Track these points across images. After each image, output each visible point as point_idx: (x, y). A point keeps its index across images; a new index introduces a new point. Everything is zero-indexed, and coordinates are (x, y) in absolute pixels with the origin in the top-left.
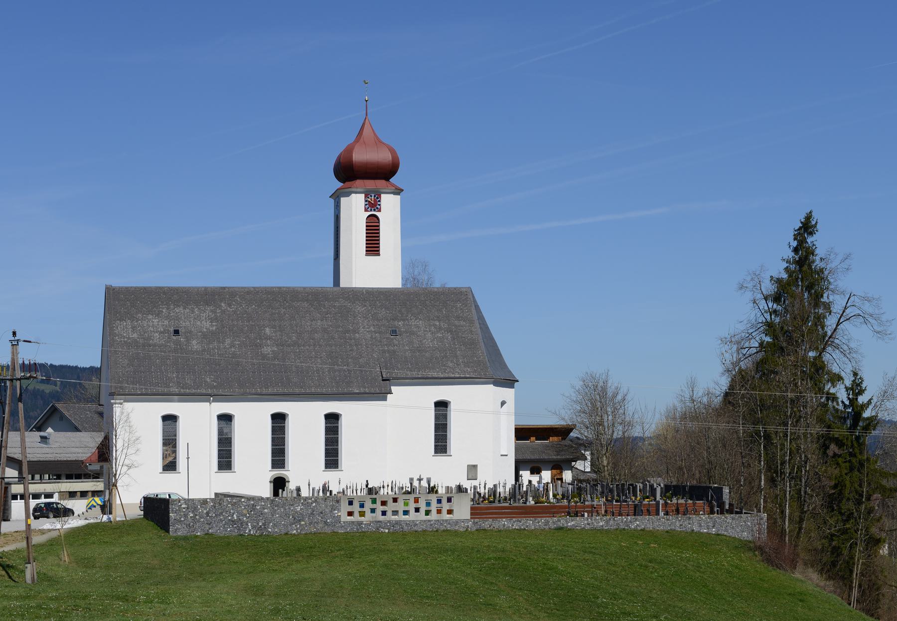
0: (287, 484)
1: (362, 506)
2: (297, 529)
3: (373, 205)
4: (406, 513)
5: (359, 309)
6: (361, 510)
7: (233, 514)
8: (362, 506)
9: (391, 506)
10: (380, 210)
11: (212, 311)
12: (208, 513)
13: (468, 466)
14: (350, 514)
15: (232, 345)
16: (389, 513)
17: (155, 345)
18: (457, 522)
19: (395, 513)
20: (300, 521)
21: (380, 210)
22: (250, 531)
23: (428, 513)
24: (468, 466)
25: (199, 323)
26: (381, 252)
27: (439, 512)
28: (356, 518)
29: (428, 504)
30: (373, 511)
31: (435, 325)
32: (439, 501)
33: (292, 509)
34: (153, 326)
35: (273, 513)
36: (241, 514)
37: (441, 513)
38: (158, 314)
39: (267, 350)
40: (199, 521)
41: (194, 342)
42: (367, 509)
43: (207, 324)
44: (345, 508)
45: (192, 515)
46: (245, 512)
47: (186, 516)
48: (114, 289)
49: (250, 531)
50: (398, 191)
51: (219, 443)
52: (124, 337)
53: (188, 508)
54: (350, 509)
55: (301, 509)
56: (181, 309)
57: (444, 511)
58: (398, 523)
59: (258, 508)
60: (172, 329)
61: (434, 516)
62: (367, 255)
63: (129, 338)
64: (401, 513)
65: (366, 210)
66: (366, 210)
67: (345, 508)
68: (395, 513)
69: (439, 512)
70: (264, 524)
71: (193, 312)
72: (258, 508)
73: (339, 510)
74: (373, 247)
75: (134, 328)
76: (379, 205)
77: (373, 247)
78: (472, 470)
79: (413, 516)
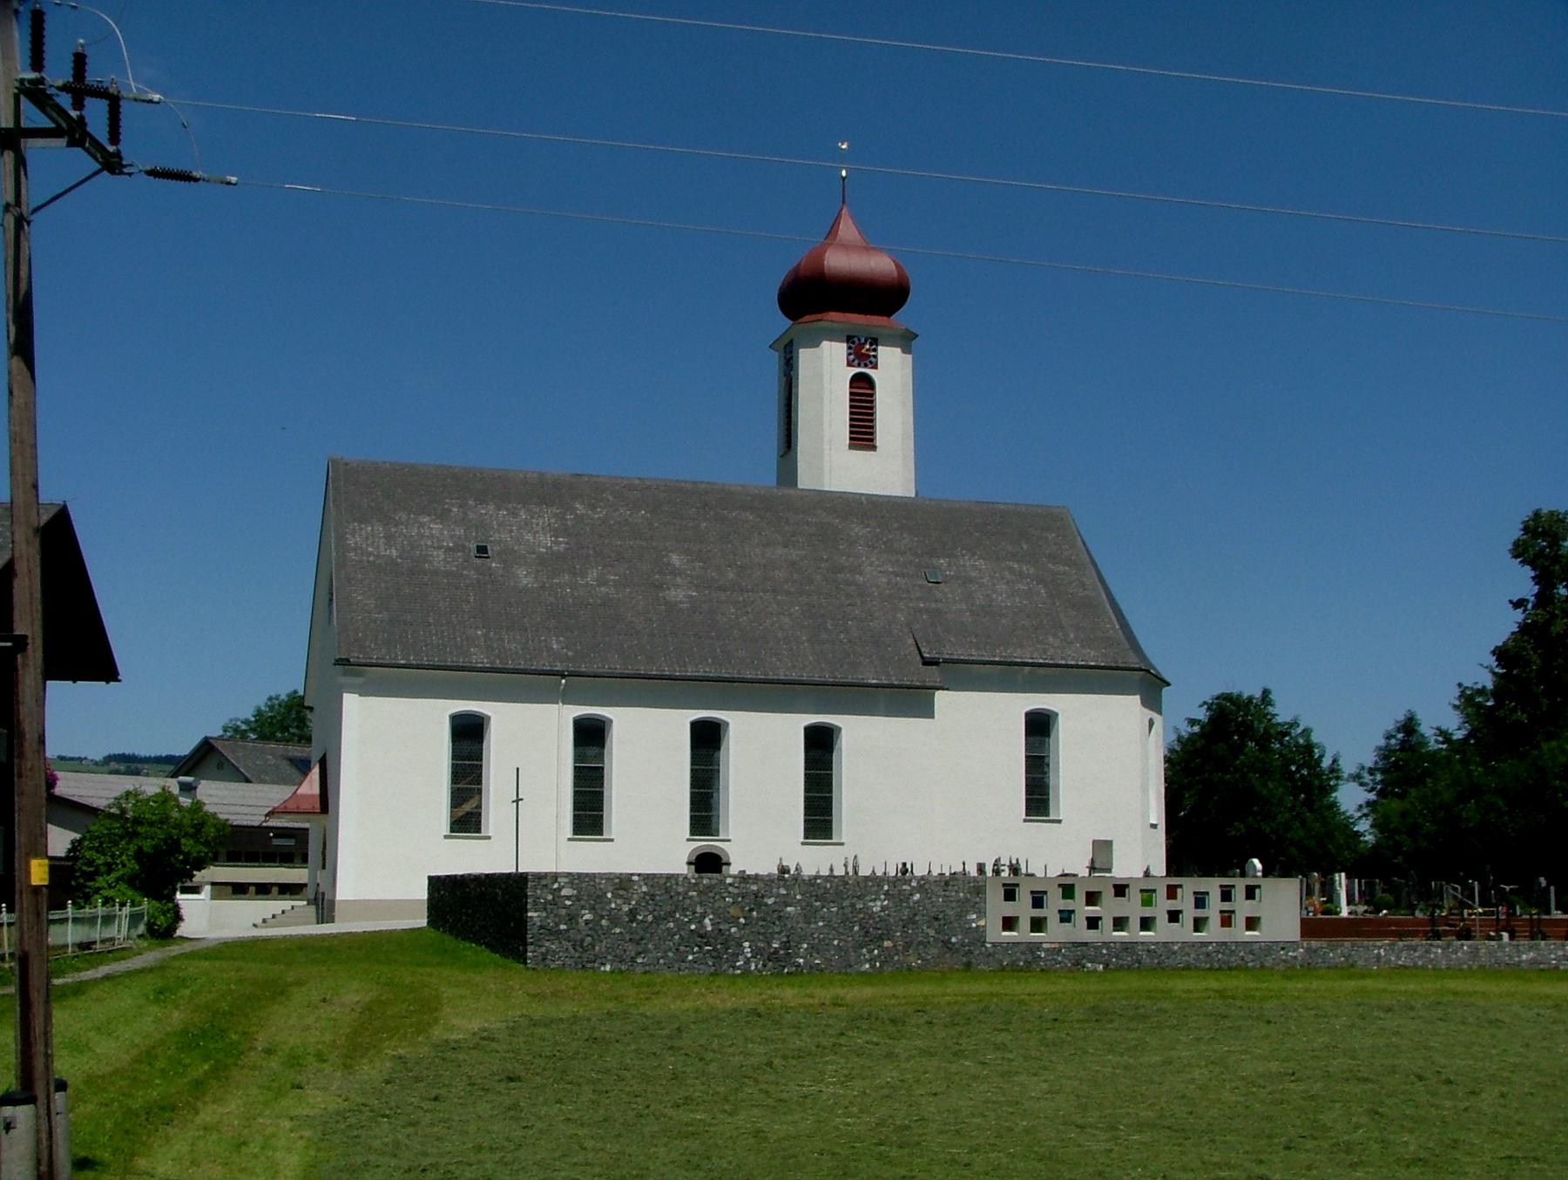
0: (724, 868)
1: (1038, 901)
2: (872, 961)
3: (861, 354)
4: (1146, 924)
5: (857, 530)
6: (1038, 913)
7: (704, 916)
8: (1038, 901)
9: (1108, 908)
10: (875, 367)
11: (556, 515)
12: (632, 914)
13: (1094, 842)
14: (1009, 923)
15: (602, 581)
16: (1107, 923)
17: (436, 572)
18: (1270, 947)
19: (1120, 923)
20: (881, 938)
21: (875, 367)
22: (747, 961)
23: (1199, 924)
24: (1094, 842)
25: (529, 537)
26: (878, 442)
27: (1227, 920)
28: (1022, 934)
29: (1200, 901)
30: (1066, 916)
31: (1010, 568)
32: (1226, 895)
33: (860, 906)
34: (432, 536)
35: (809, 915)
36: (722, 917)
37: (1230, 925)
38: (443, 516)
39: (679, 594)
40: (607, 932)
41: (522, 572)
42: (1050, 912)
43: (547, 540)
44: (997, 907)
45: (588, 917)
46: (733, 911)
47: (572, 918)
48: (346, 464)
49: (747, 961)
50: (906, 341)
51: (576, 777)
52: (370, 554)
53: (578, 898)
54: (1009, 909)
55: (883, 909)
56: (491, 507)
57: (1239, 920)
58: (1127, 947)
59: (770, 901)
60: (473, 546)
61: (1214, 932)
62: (851, 447)
63: (378, 556)
64: (1135, 923)
65: (850, 364)
66: (850, 364)
67: (997, 907)
68: (1120, 923)
69: (1227, 920)
70: (786, 945)
71: (515, 515)
72: (770, 901)
73: (982, 913)
74: (862, 433)
75: (389, 538)
76: (875, 357)
77: (862, 433)
78: (1103, 848)
79: (1164, 932)
